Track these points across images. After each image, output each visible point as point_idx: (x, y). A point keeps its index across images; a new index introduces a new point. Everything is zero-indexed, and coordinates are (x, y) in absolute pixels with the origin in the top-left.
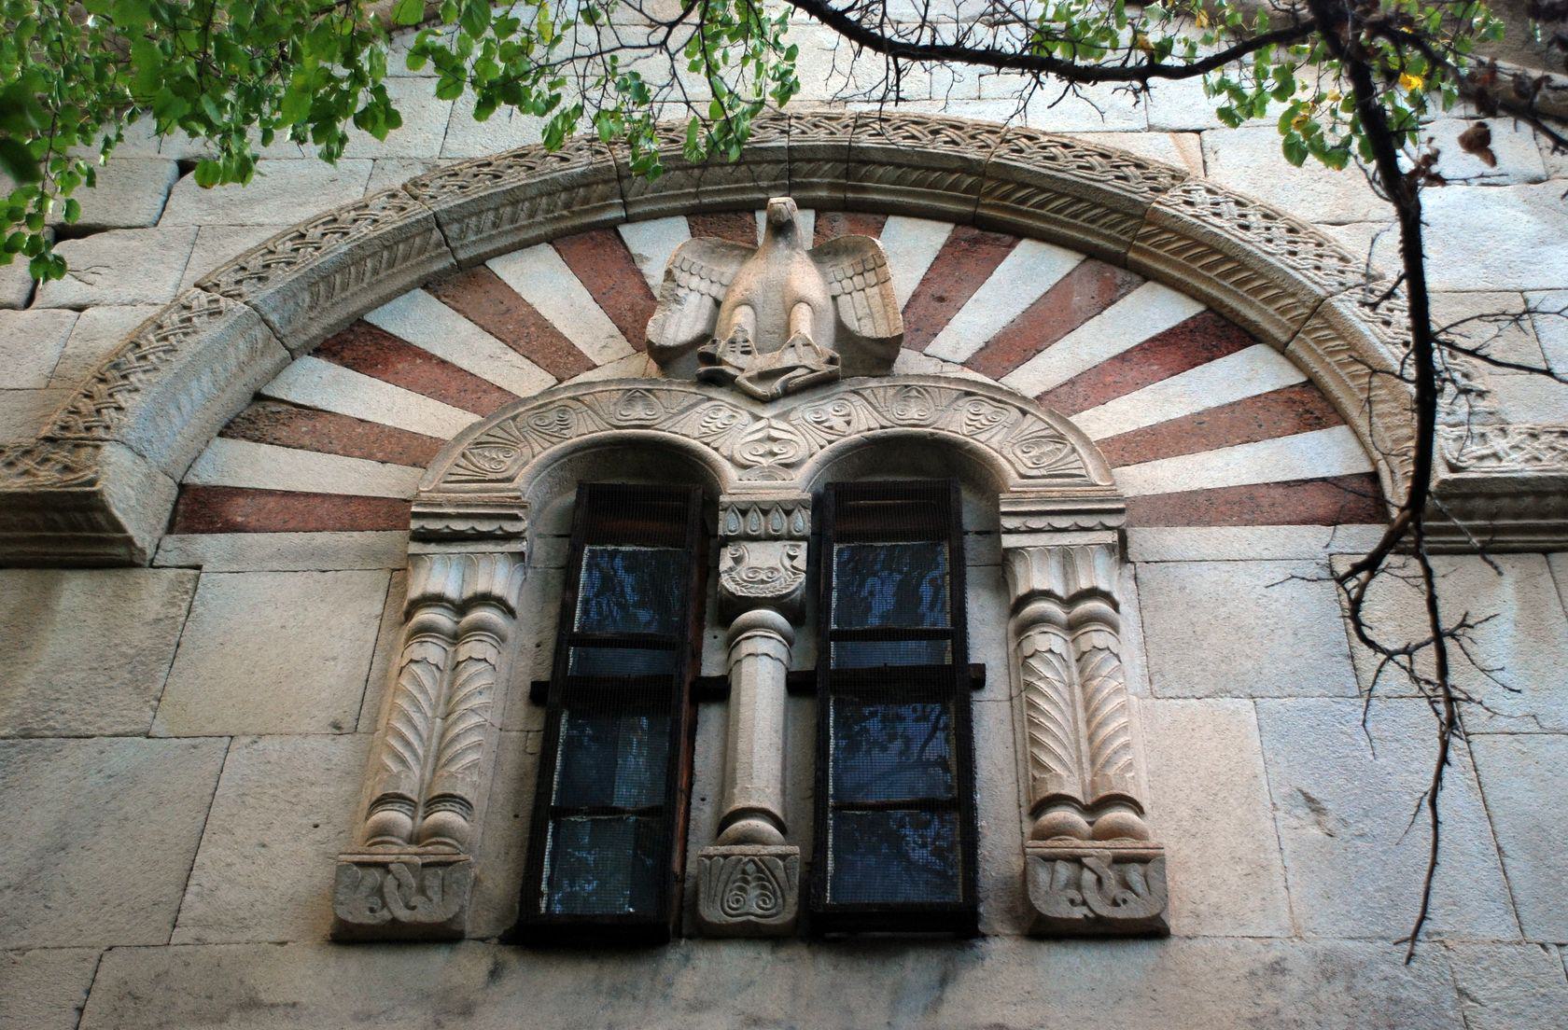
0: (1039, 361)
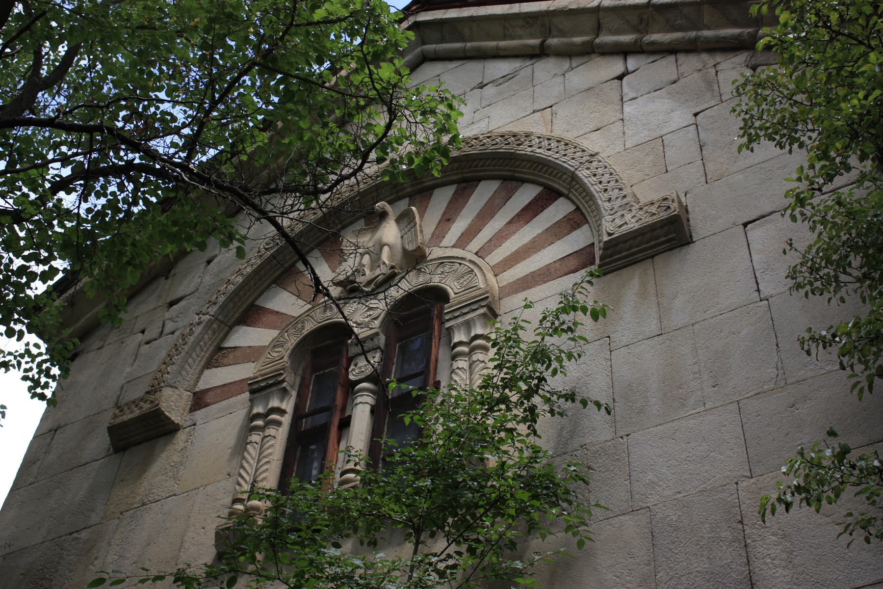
0: (480, 234)
